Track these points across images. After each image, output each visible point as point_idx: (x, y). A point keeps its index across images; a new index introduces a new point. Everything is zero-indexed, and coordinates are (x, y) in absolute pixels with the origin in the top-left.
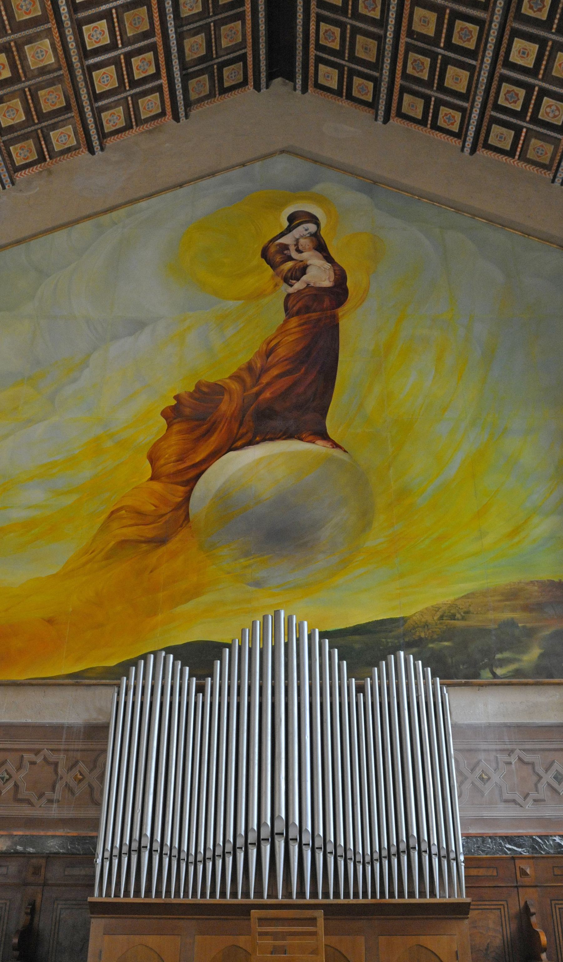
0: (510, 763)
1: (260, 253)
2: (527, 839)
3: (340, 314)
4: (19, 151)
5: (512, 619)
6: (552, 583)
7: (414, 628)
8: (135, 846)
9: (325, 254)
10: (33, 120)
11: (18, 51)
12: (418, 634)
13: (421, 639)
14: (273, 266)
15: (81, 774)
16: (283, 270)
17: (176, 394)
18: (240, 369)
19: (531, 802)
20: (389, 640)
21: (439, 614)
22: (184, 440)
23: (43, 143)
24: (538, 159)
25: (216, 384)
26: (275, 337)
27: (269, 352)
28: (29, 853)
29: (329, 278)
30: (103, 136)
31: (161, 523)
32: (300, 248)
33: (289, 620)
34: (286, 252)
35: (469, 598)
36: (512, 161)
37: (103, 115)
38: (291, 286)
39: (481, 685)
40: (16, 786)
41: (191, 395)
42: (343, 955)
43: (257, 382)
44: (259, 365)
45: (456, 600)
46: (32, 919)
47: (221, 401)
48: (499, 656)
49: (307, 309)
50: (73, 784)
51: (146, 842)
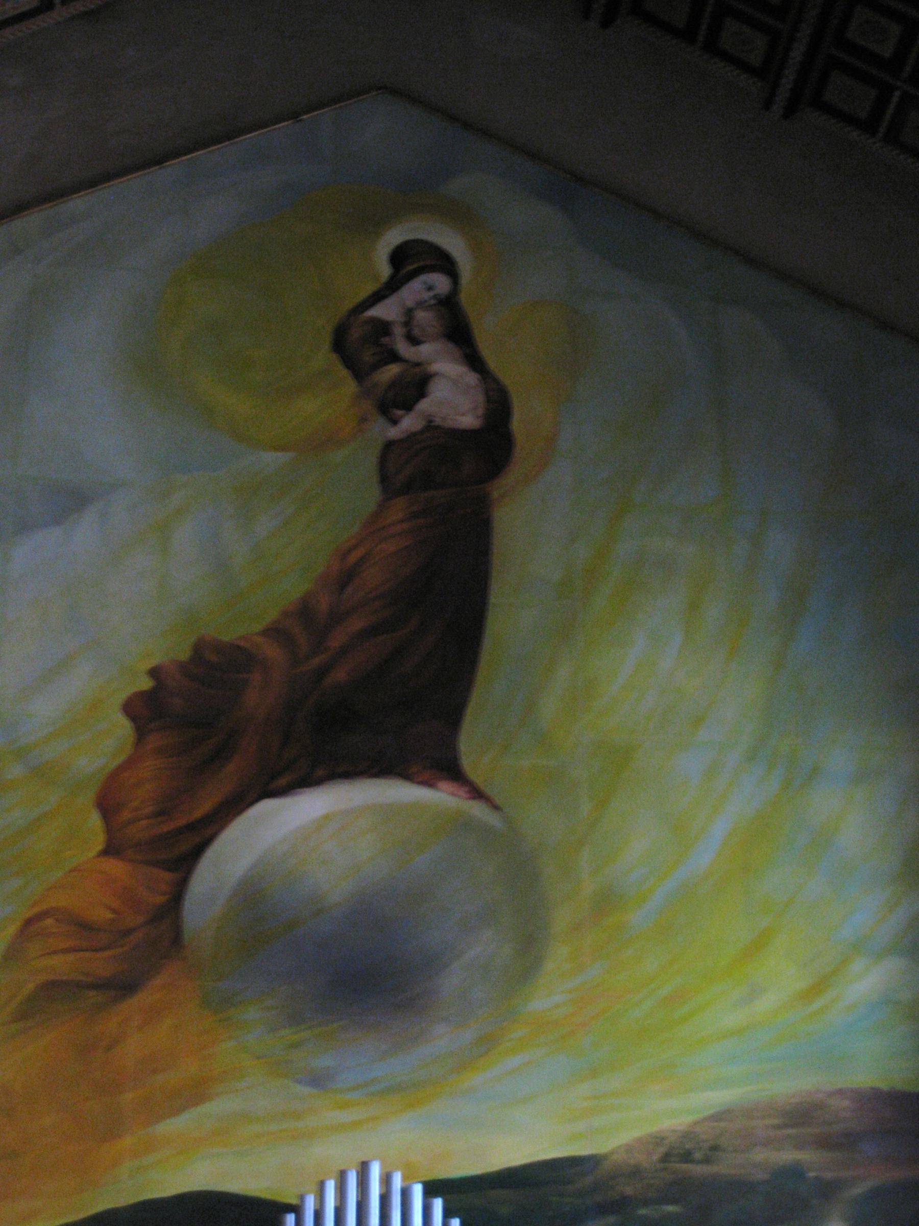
3: (495, 494)
14: (359, 372)
18: (285, 614)
21: (662, 1150)
25: (239, 647)
29: (475, 408)
32: (416, 332)
41: (183, 667)
45: (696, 1123)
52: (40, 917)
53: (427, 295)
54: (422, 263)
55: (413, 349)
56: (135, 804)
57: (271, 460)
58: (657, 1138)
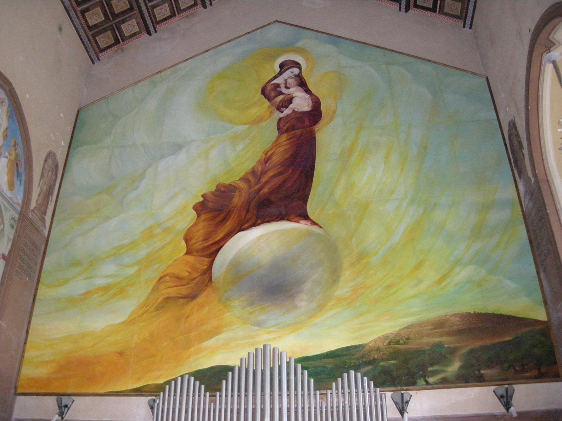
1: (260, 92)
3: (316, 130)
5: (440, 342)
6: (469, 314)
7: (370, 352)
13: (374, 359)
16: (276, 101)
17: (202, 193)
18: (247, 173)
20: (352, 361)
21: (388, 341)
22: (209, 225)
23: (117, 32)
24: (452, 13)
25: (231, 185)
26: (271, 149)
27: (267, 160)
29: (308, 105)
30: (155, 23)
31: (192, 285)
32: (288, 85)
34: (278, 89)
36: (434, 15)
37: (155, 10)
38: (282, 112)
41: (213, 194)
43: (258, 182)
44: (260, 170)
45: (400, 330)
47: (233, 196)
48: (430, 369)
49: (293, 128)
53: (292, 75)
58: (386, 336)
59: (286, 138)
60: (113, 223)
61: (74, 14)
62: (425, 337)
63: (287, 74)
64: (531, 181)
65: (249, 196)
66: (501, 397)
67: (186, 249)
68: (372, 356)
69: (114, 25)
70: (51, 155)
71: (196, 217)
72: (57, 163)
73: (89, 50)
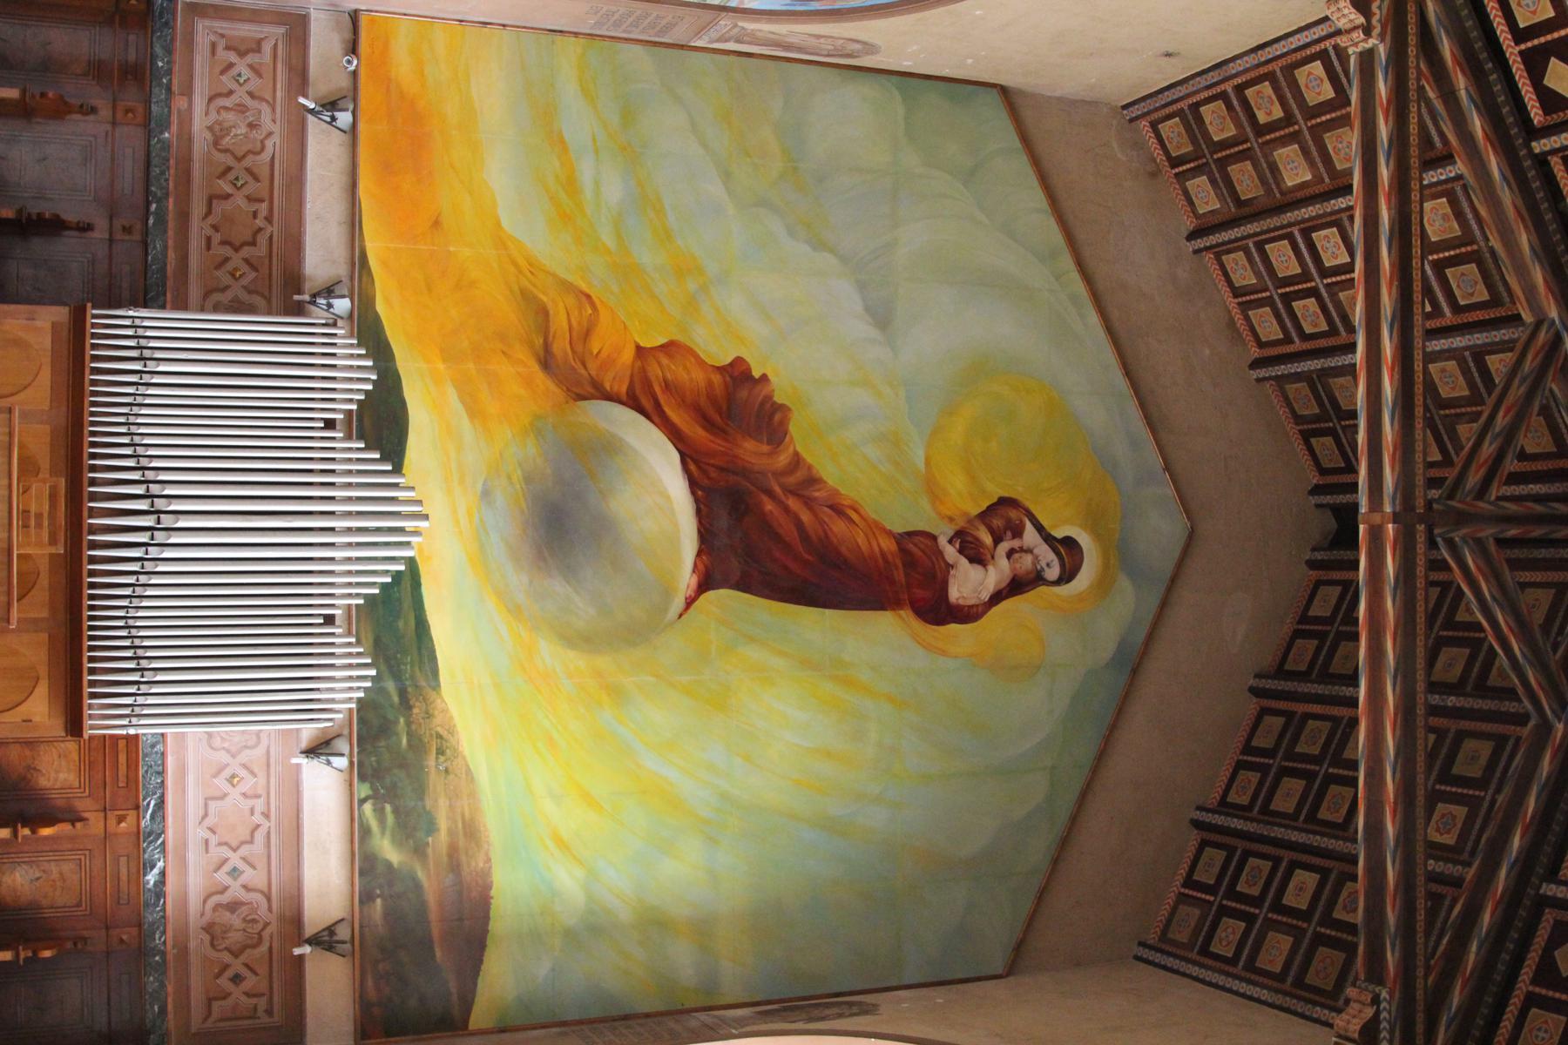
0: (252, 813)
1: (1006, 494)
2: (161, 826)
3: (902, 612)
4: (1176, 130)
5: (438, 830)
6: (488, 887)
7: (425, 700)
8: (147, 353)
9: (1004, 593)
10: (1216, 152)
11: (1290, 134)
12: (417, 704)
13: (410, 708)
14: (984, 516)
15: (241, 276)
16: (978, 529)
17: (770, 377)
18: (810, 468)
19: (206, 836)
21: (444, 734)
23: (1192, 165)
25: (786, 434)
27: (838, 509)
28: (147, 220)
31: (572, 362)
32: (1016, 556)
33: (416, 533)
35: (467, 775)
38: (950, 542)
39: (351, 785)
40: (227, 196)
41: (769, 398)
42: (28, 593)
44: (817, 494)
45: (464, 758)
46: (71, 229)
47: (761, 442)
48: (388, 808)
49: (910, 561)
50: (229, 266)
51: (151, 366)
52: (593, 305)
53: (1043, 564)
54: (1066, 560)
55: (1004, 554)
56: (673, 367)
57: (919, 456)
59: (886, 549)
60: (715, 188)
61: (1215, 80)
62: (448, 803)
63: (1046, 554)
64: (735, 1028)
65: (758, 473)
66: (331, 930)
67: (649, 345)
68: (417, 704)
69: (1204, 160)
70: (870, 48)
71: (717, 365)
72: (856, 57)
73: (1148, 101)
